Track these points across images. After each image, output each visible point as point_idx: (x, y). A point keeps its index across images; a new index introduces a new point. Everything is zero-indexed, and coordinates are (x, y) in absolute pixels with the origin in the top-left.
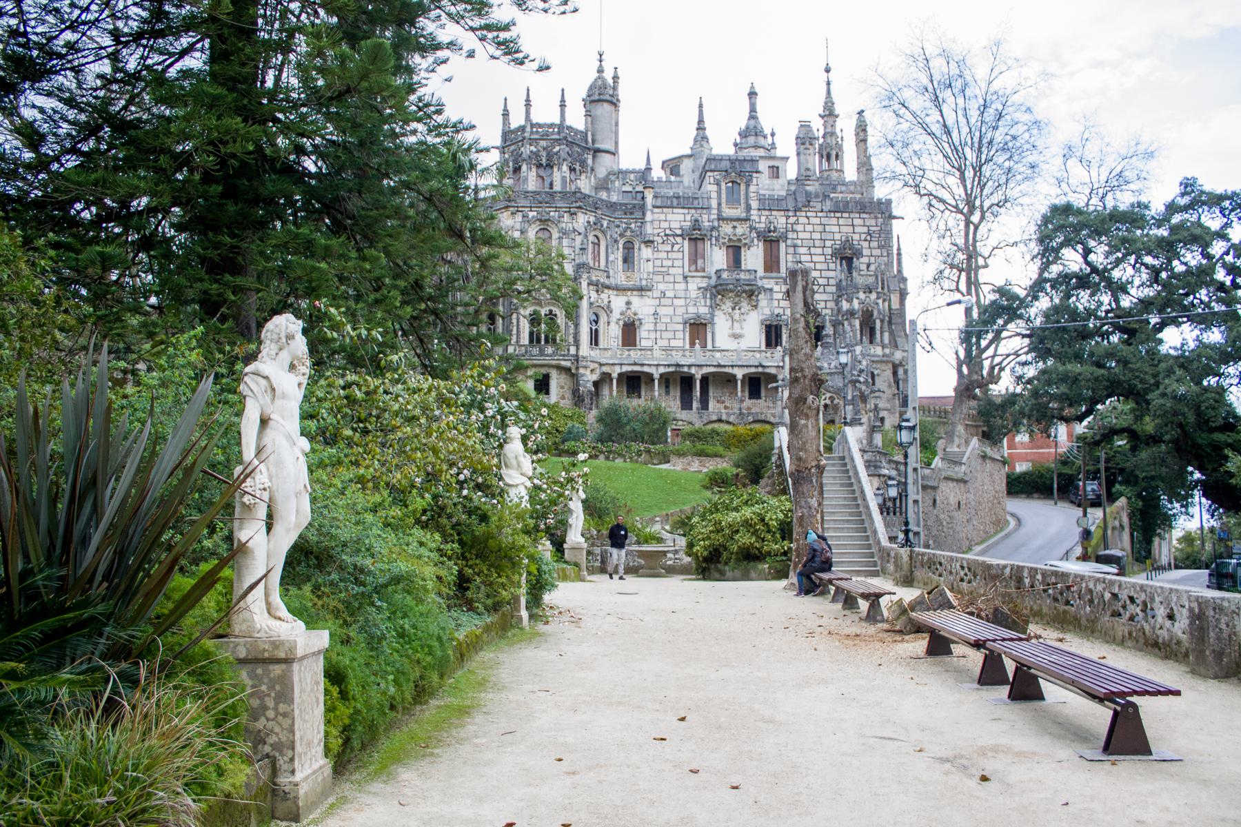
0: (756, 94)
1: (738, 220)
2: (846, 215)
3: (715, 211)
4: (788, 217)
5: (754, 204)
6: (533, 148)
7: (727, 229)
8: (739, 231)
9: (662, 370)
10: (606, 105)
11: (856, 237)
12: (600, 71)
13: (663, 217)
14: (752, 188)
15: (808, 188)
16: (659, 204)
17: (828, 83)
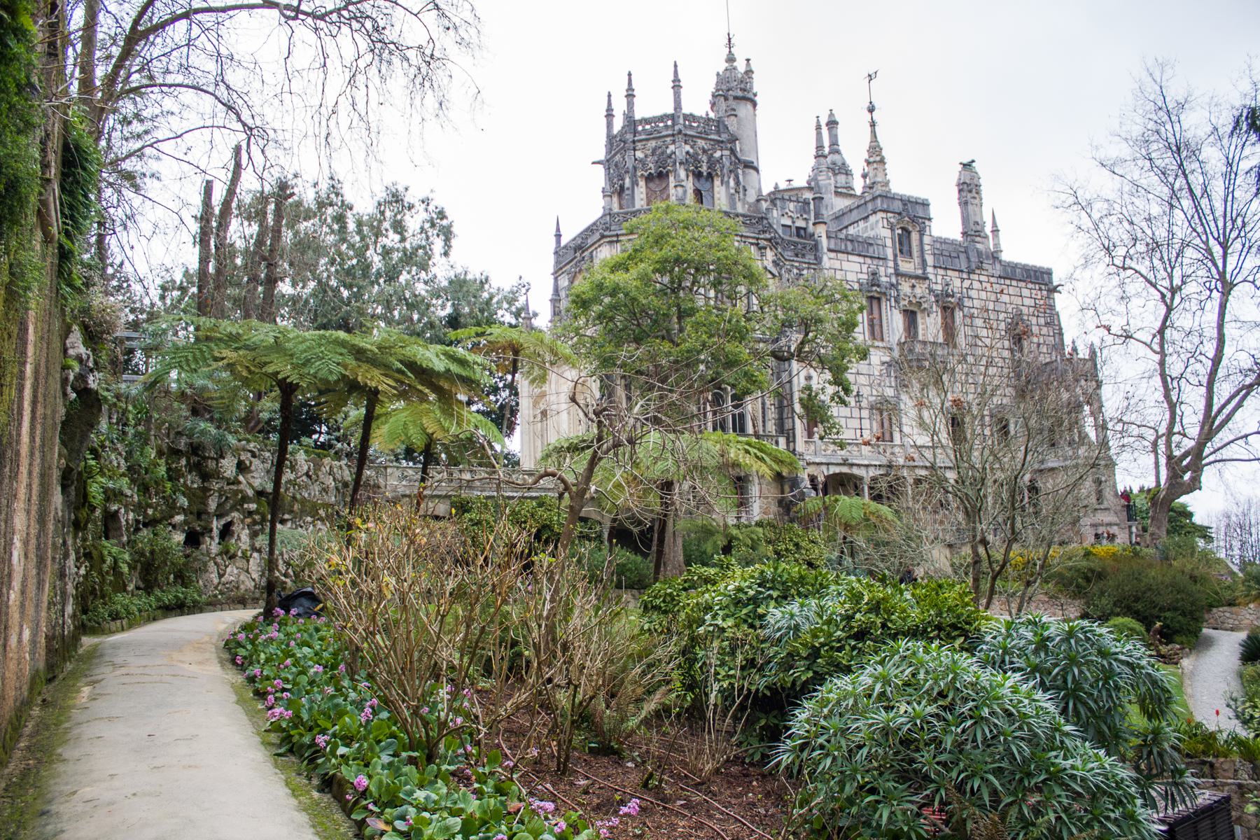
0: (836, 123)
1: (917, 277)
2: (1014, 283)
3: (891, 264)
4: (963, 280)
5: (930, 260)
6: (688, 148)
7: (905, 287)
8: (919, 291)
9: (873, 472)
10: (749, 106)
11: (1025, 310)
12: (731, 59)
13: (837, 264)
14: (926, 239)
15: (978, 246)
16: (832, 247)
17: (873, 124)
